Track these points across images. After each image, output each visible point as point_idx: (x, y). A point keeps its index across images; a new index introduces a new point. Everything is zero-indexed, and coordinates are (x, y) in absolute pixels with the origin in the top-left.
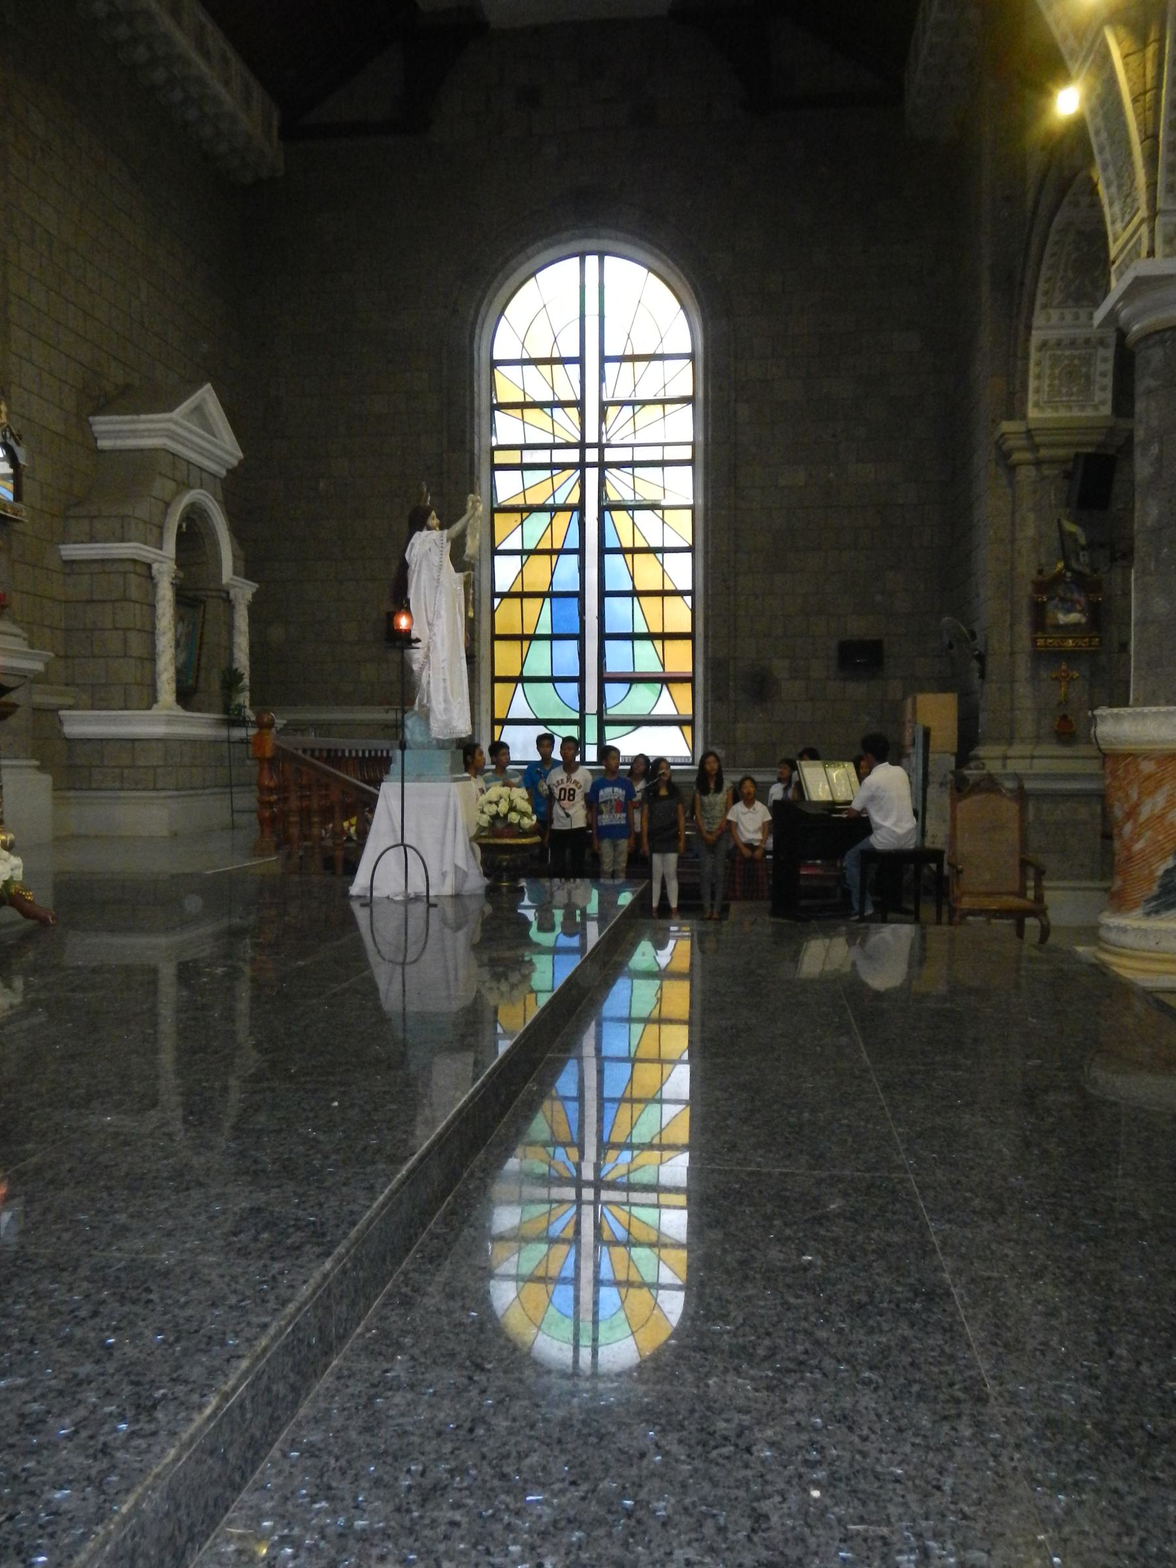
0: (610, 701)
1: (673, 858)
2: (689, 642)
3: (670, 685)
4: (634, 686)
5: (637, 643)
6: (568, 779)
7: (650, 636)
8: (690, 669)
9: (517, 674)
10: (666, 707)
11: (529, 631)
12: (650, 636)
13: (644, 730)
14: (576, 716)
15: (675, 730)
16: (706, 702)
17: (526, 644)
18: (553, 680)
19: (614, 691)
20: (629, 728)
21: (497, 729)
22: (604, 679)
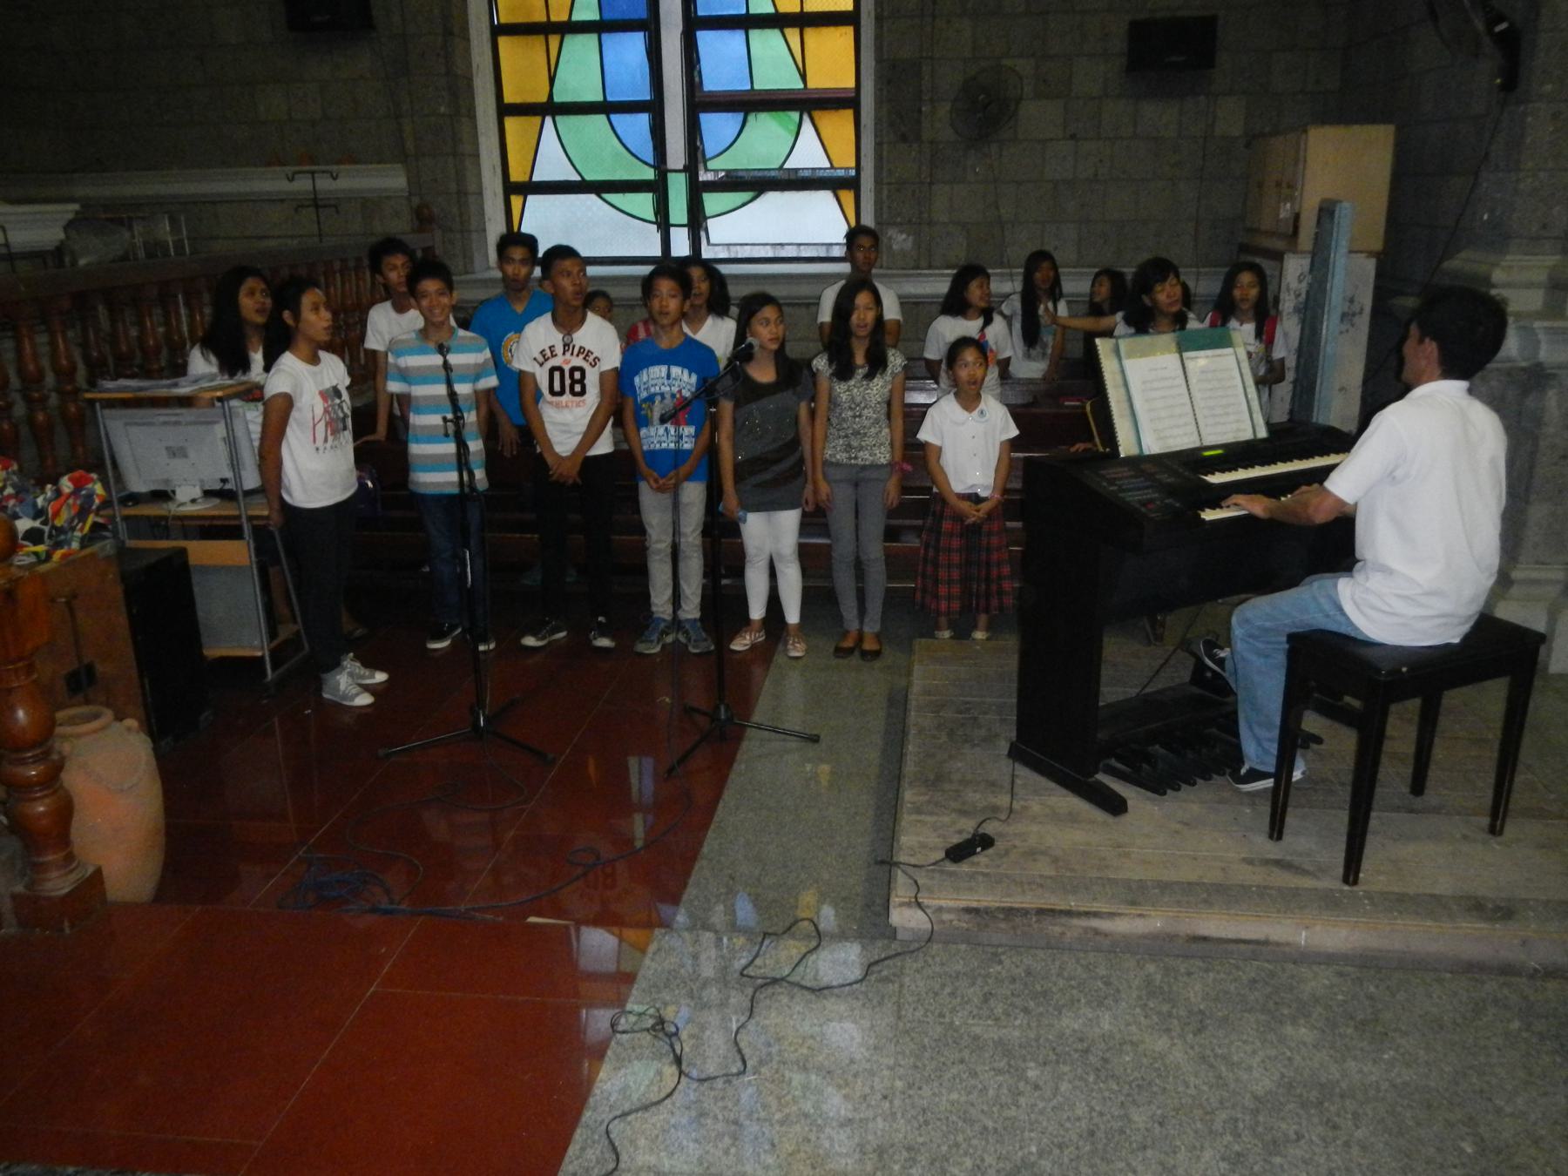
0: (710, 144)
1: (789, 520)
2: (848, 31)
3: (816, 114)
4: (751, 117)
5: (755, 34)
6: (566, 346)
7: (777, 21)
8: (851, 84)
9: (544, 99)
10: (809, 154)
11: (559, 16)
12: (777, 21)
13: (772, 199)
14: (649, 174)
15: (825, 198)
16: (879, 145)
17: (554, 41)
18: (606, 108)
19: (717, 127)
20: (746, 196)
21: (516, 201)
22: (699, 102)
